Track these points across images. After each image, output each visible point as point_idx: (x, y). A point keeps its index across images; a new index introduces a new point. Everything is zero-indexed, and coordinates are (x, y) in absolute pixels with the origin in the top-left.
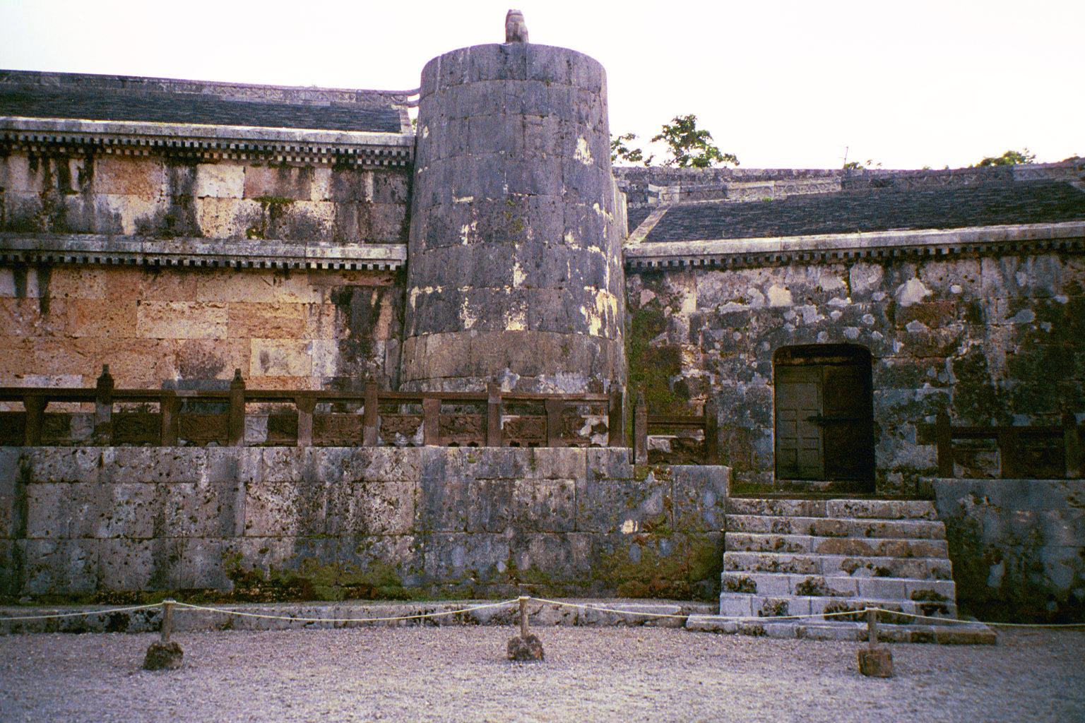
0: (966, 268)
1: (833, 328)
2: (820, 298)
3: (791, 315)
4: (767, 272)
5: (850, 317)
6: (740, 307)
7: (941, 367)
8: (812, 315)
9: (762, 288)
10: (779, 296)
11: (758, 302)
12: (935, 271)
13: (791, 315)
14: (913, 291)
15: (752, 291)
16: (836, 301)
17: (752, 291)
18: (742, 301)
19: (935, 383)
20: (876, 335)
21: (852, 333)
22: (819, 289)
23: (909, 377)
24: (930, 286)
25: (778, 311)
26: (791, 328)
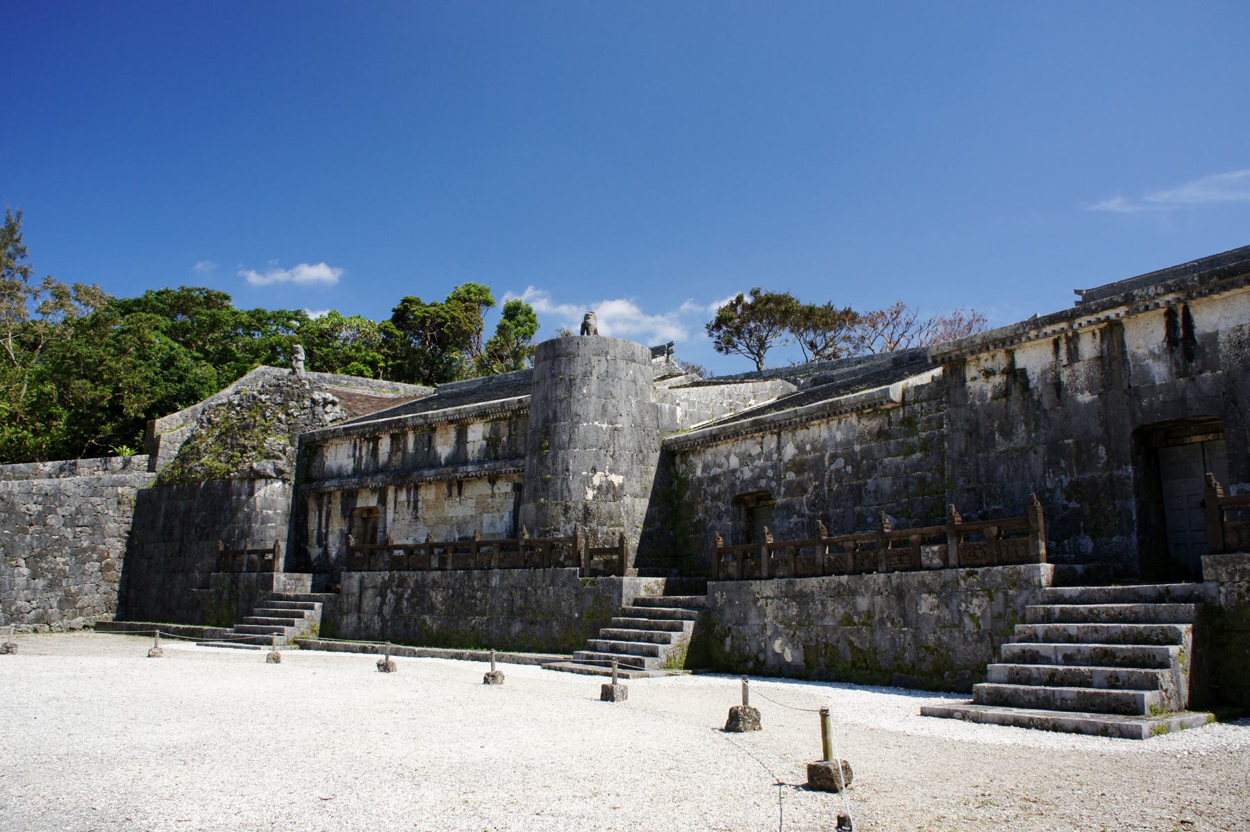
1: (755, 480)
3: (738, 474)
6: (719, 470)
7: (801, 504)
8: (747, 474)
10: (734, 462)
11: (725, 468)
12: (801, 434)
14: (790, 451)
16: (757, 463)
20: (774, 484)
21: (763, 483)
23: (788, 509)
24: (797, 447)
25: (734, 471)
26: (738, 482)
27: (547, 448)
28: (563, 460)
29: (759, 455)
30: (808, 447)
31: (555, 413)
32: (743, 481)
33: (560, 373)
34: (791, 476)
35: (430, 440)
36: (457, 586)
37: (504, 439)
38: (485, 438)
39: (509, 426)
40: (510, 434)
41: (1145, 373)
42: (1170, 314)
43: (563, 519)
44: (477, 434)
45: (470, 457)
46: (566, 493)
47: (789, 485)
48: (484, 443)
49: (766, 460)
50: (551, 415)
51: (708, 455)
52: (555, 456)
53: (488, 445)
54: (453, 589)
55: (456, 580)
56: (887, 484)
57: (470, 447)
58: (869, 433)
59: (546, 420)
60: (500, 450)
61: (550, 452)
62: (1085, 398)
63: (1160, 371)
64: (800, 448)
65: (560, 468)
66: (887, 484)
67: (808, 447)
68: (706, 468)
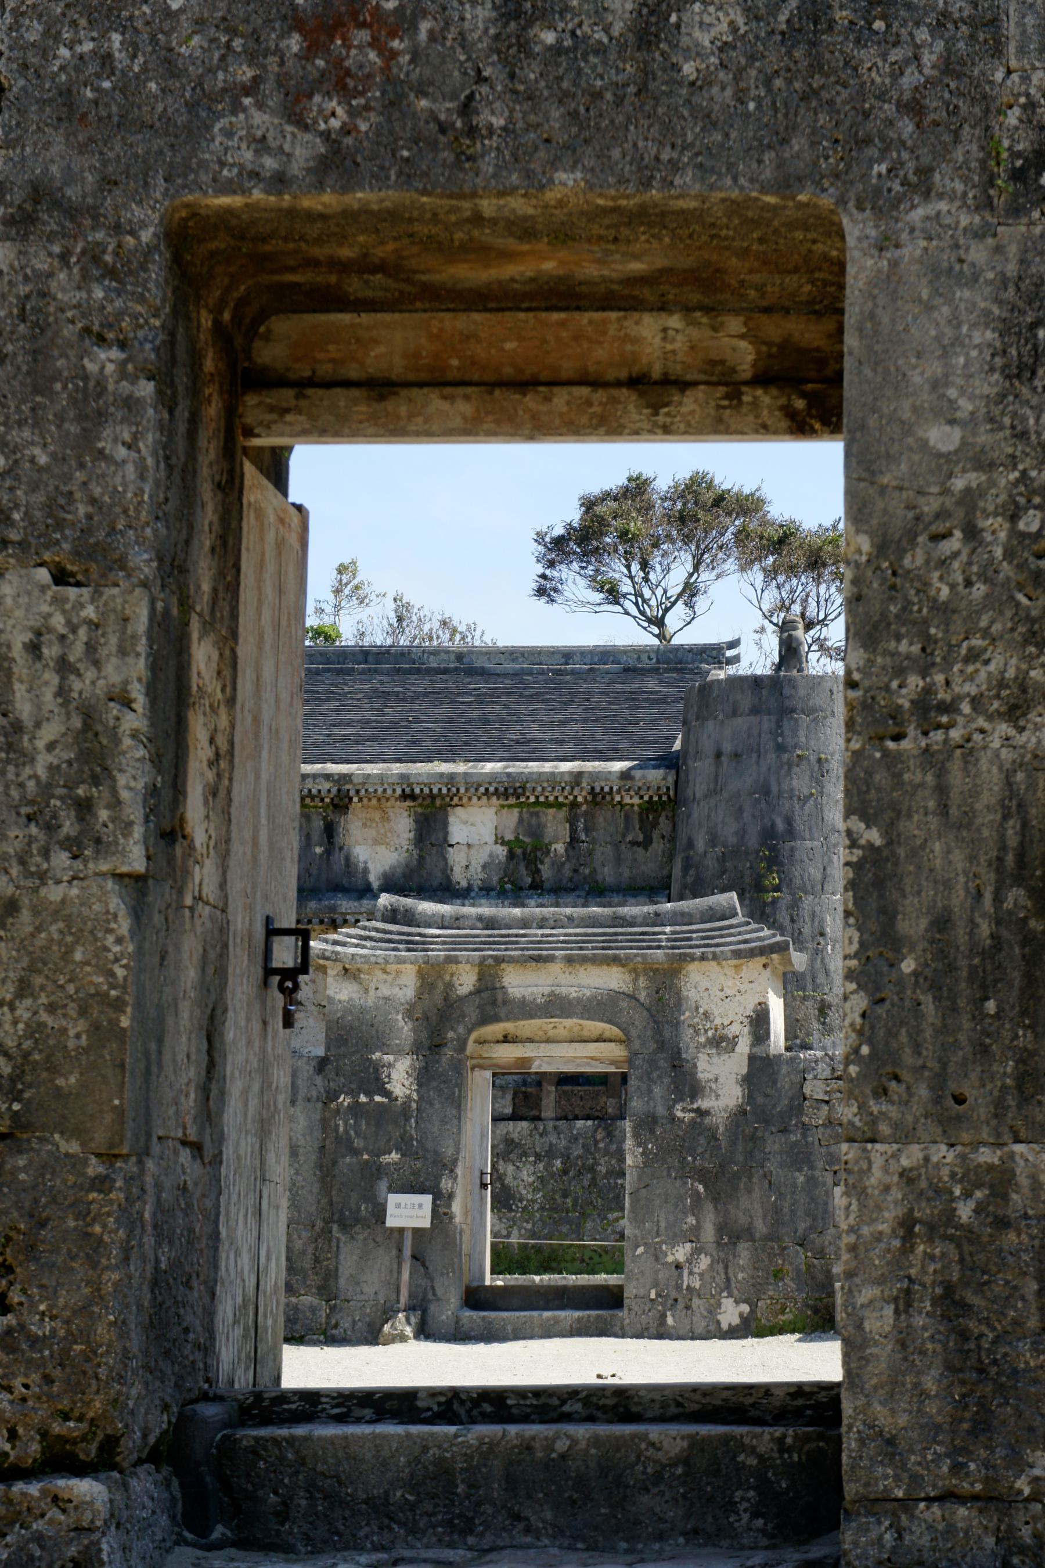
27: (777, 889)
28: (813, 915)
31: (789, 821)
33: (796, 746)
35: (330, 830)
36: (577, 1151)
37: (560, 847)
38: (500, 840)
39: (572, 821)
40: (574, 841)
43: (816, 1025)
44: (476, 834)
45: (459, 877)
46: (821, 979)
48: (501, 851)
50: (781, 825)
52: (795, 904)
53: (511, 855)
54: (566, 1158)
55: (575, 1139)
57: (457, 858)
59: (769, 834)
60: (546, 871)
61: (784, 898)
65: (807, 930)
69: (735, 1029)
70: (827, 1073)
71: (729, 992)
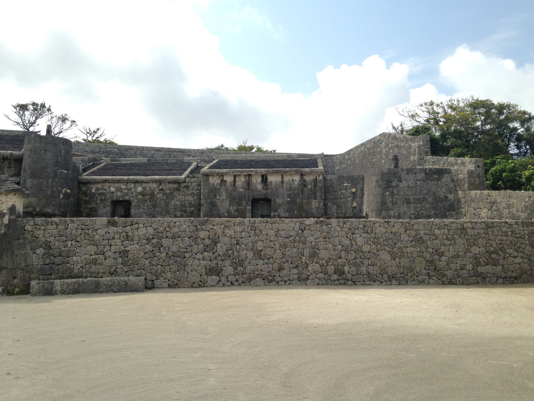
0: (151, 185)
2: (120, 190)
3: (115, 193)
4: (110, 184)
5: (127, 194)
6: (104, 191)
7: (144, 206)
8: (119, 194)
9: (109, 187)
10: (113, 189)
11: (108, 190)
12: (144, 185)
13: (115, 193)
14: (140, 189)
15: (107, 188)
17: (107, 188)
18: (105, 190)
19: (143, 209)
20: (132, 198)
21: (127, 198)
22: (121, 188)
25: (113, 193)
29: (125, 189)
30: (148, 189)
32: (117, 196)
34: (140, 197)
41: (256, 186)
42: (263, 176)
47: (139, 200)
49: (128, 190)
51: (100, 186)
56: (178, 203)
58: (173, 188)
62: (241, 190)
63: (260, 187)
64: (144, 189)
66: (178, 203)
67: (148, 189)
68: (97, 189)
69: (5, 211)
70: (32, 224)
71: (3, 201)
